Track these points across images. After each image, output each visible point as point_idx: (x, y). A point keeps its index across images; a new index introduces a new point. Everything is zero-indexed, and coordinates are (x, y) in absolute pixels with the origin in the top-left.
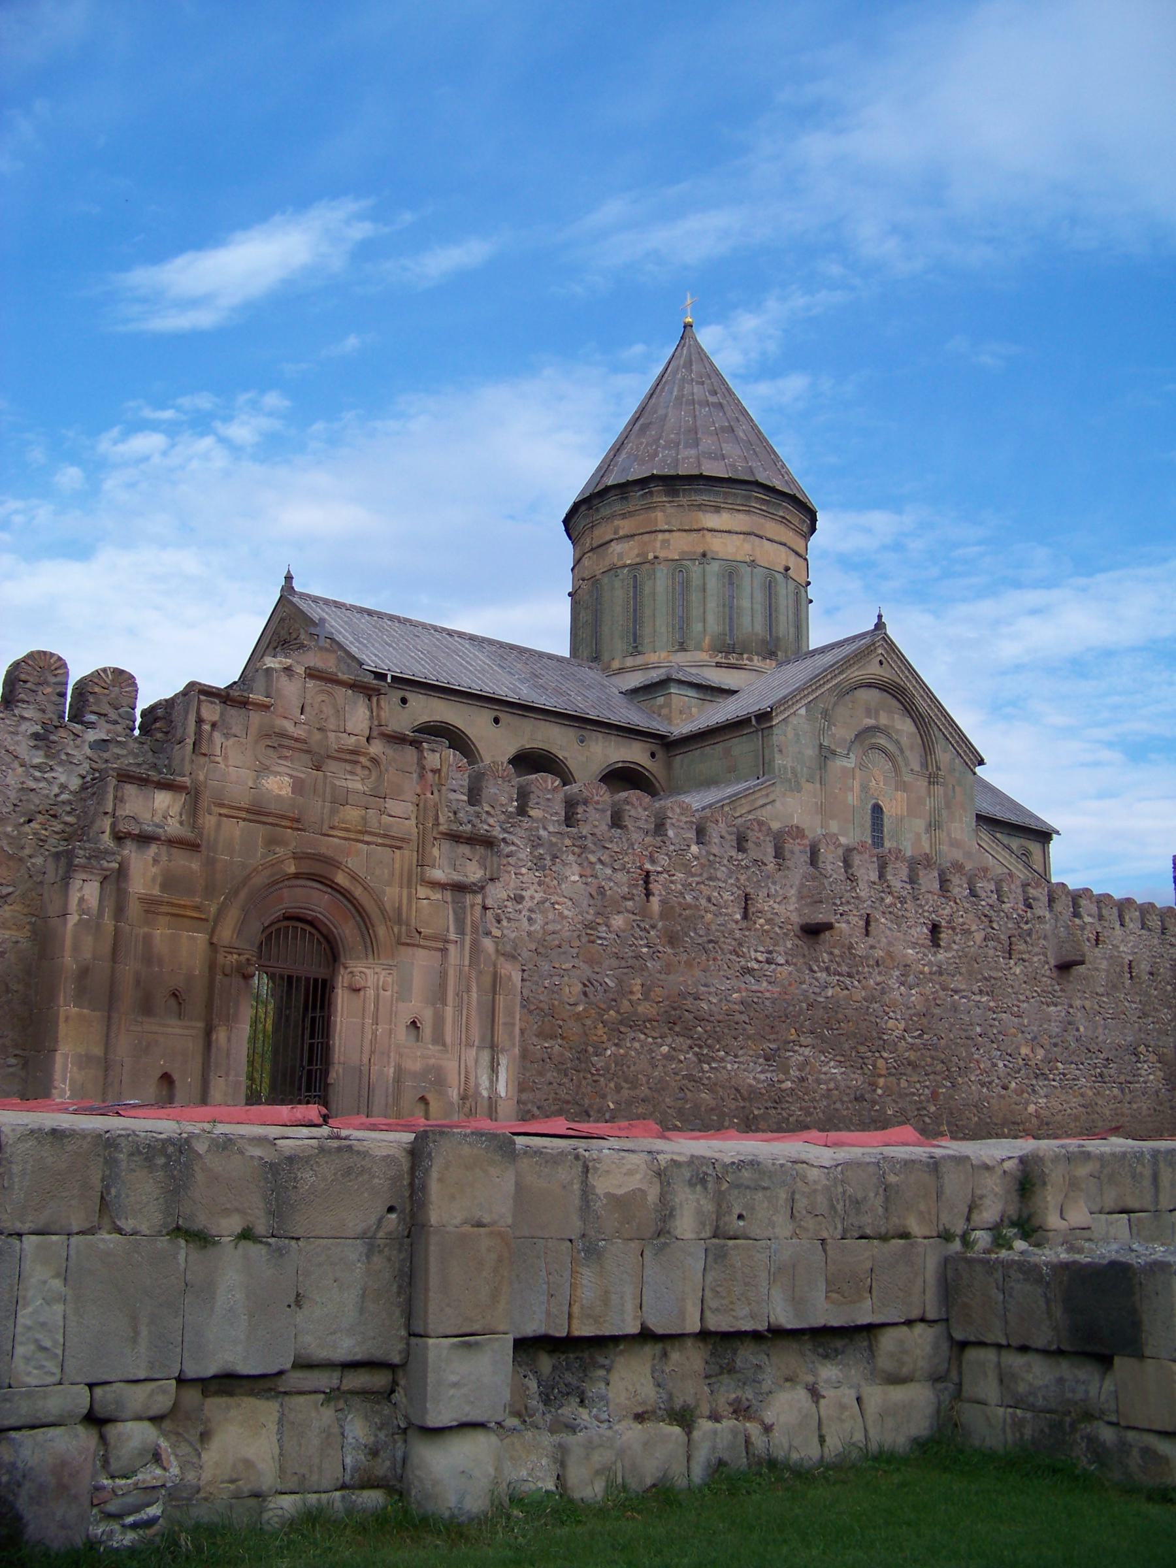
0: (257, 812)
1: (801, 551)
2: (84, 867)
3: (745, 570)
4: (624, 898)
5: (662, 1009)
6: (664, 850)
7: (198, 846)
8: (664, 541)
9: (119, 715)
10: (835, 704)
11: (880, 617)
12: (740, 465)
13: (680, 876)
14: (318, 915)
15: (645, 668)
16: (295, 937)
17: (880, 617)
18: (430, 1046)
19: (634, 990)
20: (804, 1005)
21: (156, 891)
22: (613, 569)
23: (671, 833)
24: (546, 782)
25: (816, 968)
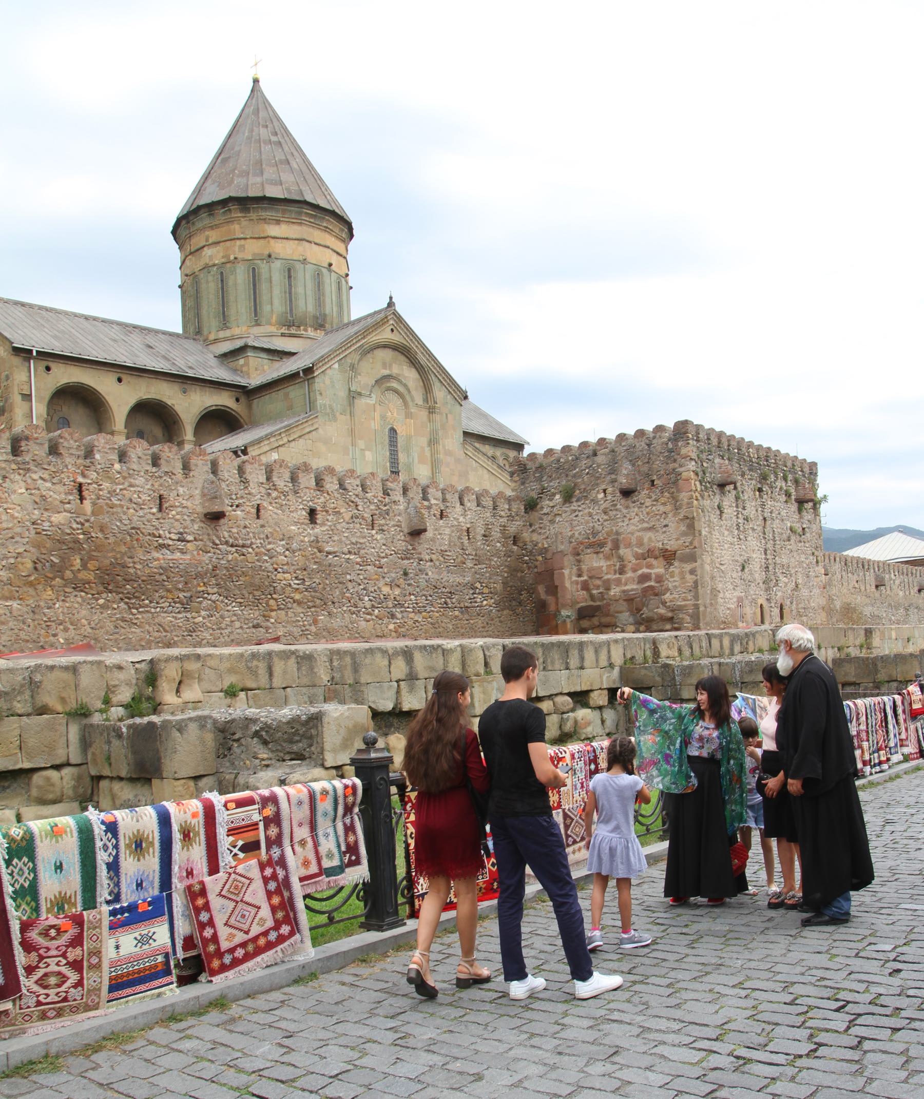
1: (342, 251)
3: (299, 266)
6: (93, 468)
10: (360, 360)
11: (391, 298)
12: (294, 188)
13: (106, 485)
15: (232, 338)
17: (391, 298)
20: (210, 567)
23: (98, 456)
25: (218, 542)
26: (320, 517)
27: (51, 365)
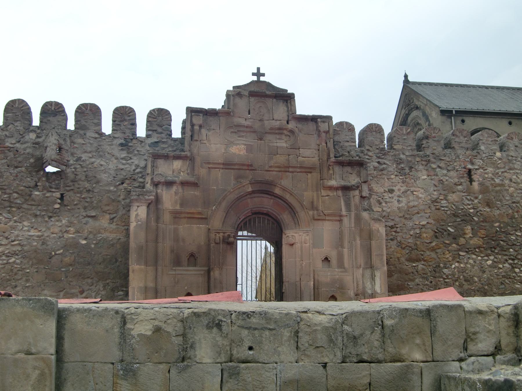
0: (228, 165)
2: (136, 200)
4: (455, 184)
5: (486, 241)
6: (479, 156)
7: (197, 184)
9: (163, 130)
13: (490, 169)
14: (269, 210)
16: (259, 222)
18: (336, 270)
19: (467, 232)
21: (178, 207)
23: (482, 148)
24: (402, 130)
27: (464, 118)
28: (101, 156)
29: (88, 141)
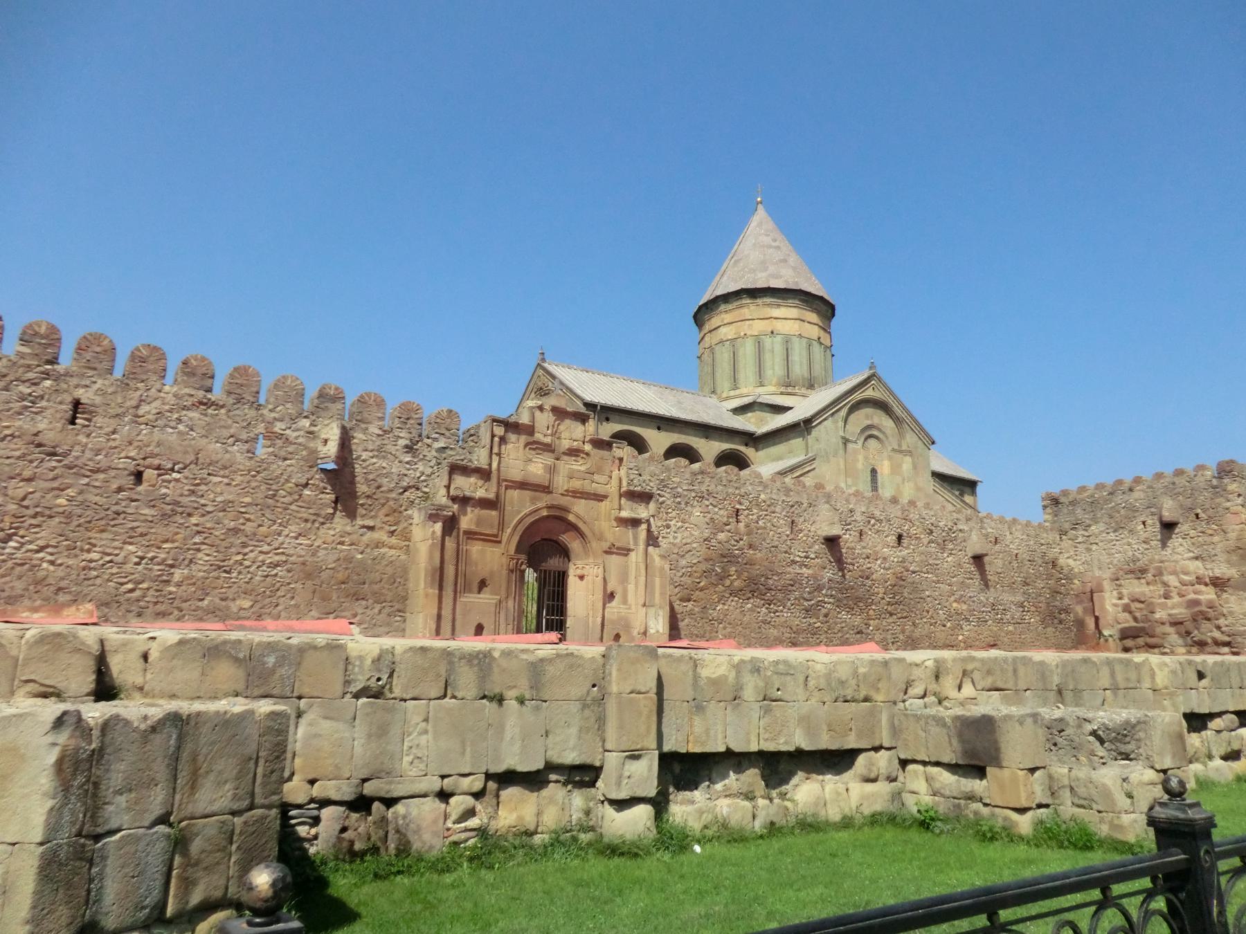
8: (750, 325)
12: (791, 280)
22: (722, 342)
26: (905, 542)
28: (384, 457)
29: (370, 437)
